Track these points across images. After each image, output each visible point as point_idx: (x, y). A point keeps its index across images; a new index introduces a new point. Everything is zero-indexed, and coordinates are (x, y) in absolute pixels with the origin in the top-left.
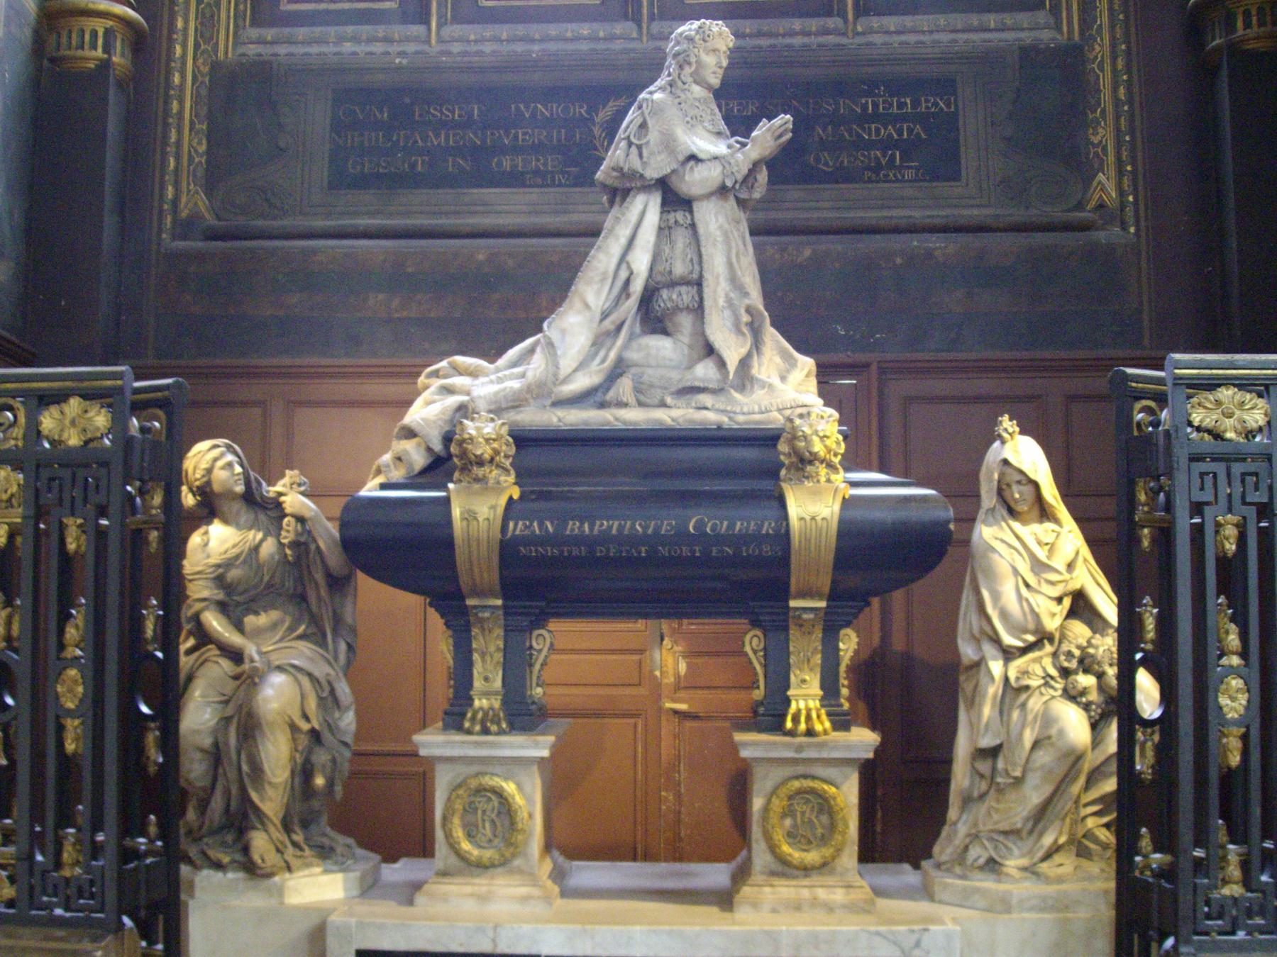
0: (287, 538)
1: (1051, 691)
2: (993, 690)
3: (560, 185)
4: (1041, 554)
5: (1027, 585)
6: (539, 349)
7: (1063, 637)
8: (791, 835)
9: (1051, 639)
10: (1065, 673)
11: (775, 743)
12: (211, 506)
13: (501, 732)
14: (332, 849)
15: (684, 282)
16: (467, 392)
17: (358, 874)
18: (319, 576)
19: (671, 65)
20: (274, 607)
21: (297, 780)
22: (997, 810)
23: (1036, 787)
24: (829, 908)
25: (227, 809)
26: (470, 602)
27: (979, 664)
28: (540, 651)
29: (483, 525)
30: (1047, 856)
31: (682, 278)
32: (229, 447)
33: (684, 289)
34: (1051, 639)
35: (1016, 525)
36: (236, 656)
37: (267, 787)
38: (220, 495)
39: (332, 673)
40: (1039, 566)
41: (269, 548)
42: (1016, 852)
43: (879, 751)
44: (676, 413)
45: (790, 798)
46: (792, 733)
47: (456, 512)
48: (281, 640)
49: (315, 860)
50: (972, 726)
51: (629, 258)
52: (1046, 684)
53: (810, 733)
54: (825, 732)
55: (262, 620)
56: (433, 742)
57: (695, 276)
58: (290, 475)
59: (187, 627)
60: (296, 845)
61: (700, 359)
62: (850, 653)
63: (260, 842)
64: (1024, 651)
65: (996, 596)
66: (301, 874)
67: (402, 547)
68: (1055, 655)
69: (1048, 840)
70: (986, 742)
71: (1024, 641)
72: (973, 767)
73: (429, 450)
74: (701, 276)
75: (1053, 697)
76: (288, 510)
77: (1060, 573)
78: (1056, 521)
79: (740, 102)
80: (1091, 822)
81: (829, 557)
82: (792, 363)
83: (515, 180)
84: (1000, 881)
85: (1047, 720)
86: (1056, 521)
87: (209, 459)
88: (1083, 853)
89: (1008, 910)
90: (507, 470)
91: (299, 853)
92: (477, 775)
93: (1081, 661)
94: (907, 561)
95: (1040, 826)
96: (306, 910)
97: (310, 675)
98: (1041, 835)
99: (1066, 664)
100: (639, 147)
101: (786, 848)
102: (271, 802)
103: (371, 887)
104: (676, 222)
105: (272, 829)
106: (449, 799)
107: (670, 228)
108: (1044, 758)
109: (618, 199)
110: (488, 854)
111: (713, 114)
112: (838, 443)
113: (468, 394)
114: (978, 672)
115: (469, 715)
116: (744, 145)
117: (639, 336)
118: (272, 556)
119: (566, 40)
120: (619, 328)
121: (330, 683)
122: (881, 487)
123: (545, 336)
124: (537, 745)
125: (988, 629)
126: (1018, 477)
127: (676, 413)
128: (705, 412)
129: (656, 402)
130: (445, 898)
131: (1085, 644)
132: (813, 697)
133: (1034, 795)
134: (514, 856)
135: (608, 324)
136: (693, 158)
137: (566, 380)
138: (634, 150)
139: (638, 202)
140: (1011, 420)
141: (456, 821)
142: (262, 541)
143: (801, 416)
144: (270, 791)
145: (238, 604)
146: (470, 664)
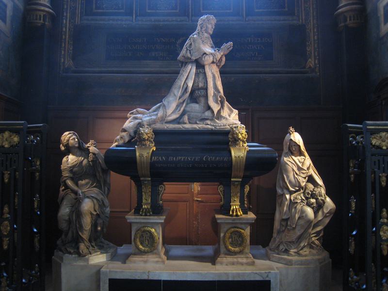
0: (90, 159)
3: (168, 60)
4: (300, 165)
5: (296, 174)
6: (161, 107)
7: (306, 188)
8: (231, 244)
9: (302, 188)
10: (307, 198)
11: (227, 219)
12: (69, 150)
13: (150, 215)
14: (103, 246)
15: (202, 88)
16: (140, 119)
17: (110, 254)
18: (100, 169)
19: (199, 28)
20: (87, 179)
21: (93, 228)
22: (287, 236)
23: (299, 230)
24: (242, 264)
25: (73, 236)
26: (142, 179)
27: (283, 195)
28: (161, 191)
29: (145, 158)
30: (302, 249)
31: (202, 87)
32: (74, 134)
33: (202, 91)
34: (302, 188)
35: (293, 157)
36: (76, 193)
37: (84, 231)
38: (71, 147)
39: (102, 197)
40: (300, 169)
41: (85, 162)
42: (293, 247)
43: (256, 220)
44: (200, 126)
45: (231, 233)
46: (232, 216)
47: (138, 154)
48: (89, 188)
49: (98, 250)
50: (280, 213)
51: (187, 82)
52: (302, 202)
53: (237, 215)
54: (241, 215)
55: (83, 182)
56: (131, 218)
57: (205, 87)
58: (91, 141)
59: (62, 184)
60: (92, 246)
61: (207, 111)
62: (247, 192)
63: (82, 246)
64: (295, 192)
65: (288, 177)
66: (94, 254)
67: (121, 162)
68: (304, 193)
69: (302, 245)
70: (285, 217)
71: (295, 189)
72: (281, 222)
73: (130, 135)
74: (207, 87)
76: (91, 151)
77: (305, 170)
79: (218, 40)
80: (313, 239)
81: (243, 167)
82: (232, 111)
83: (155, 59)
84: (289, 256)
85: (302, 211)
87: (68, 137)
88: (311, 247)
89: (292, 265)
90: (152, 142)
91: (93, 249)
92: (144, 227)
93: (311, 195)
94: (265, 167)
95: (300, 240)
96: (94, 266)
97: (96, 199)
98: (300, 243)
100: (190, 50)
101: (230, 247)
102: (85, 235)
103: (114, 256)
104: (200, 72)
105: (85, 242)
106: (136, 234)
107: (198, 73)
108: (302, 222)
109: (184, 65)
110: (147, 249)
111: (210, 41)
112: (245, 135)
113: (141, 119)
114: (283, 197)
115: (141, 210)
116: (219, 50)
117: (190, 103)
118: (86, 164)
119: (169, 21)
120: (184, 101)
121: (102, 200)
122: (256, 147)
123: (163, 104)
124: (160, 219)
125: (286, 186)
127: (200, 126)
128: (208, 126)
129: (194, 122)
130: (135, 262)
132: (237, 205)
133: (298, 233)
134: (154, 250)
135: (181, 100)
136: (205, 53)
137: (170, 116)
138: (188, 51)
139: (189, 67)
141: (138, 240)
142: (83, 160)
143: (235, 127)
144: (85, 232)
145: (77, 178)
146: (142, 195)
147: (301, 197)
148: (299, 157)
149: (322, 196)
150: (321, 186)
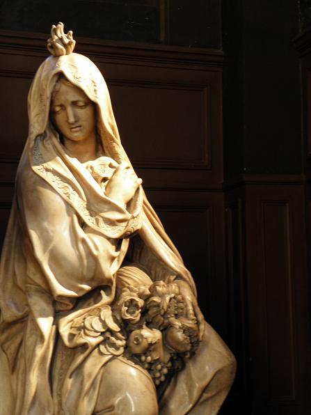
1: (112, 350)
2: (42, 351)
4: (100, 189)
5: (83, 225)
10: (126, 327)
40: (96, 203)
64: (77, 303)
65: (46, 240)
75: (114, 357)
77: (121, 211)
78: (114, 156)
85: (107, 386)
86: (114, 156)
93: (145, 312)
99: (128, 317)
114: (24, 329)
126: (73, 96)
131: (148, 292)
140: (66, 31)
147: (104, 322)
148: (91, 163)
149: (187, 316)
150: (179, 277)
